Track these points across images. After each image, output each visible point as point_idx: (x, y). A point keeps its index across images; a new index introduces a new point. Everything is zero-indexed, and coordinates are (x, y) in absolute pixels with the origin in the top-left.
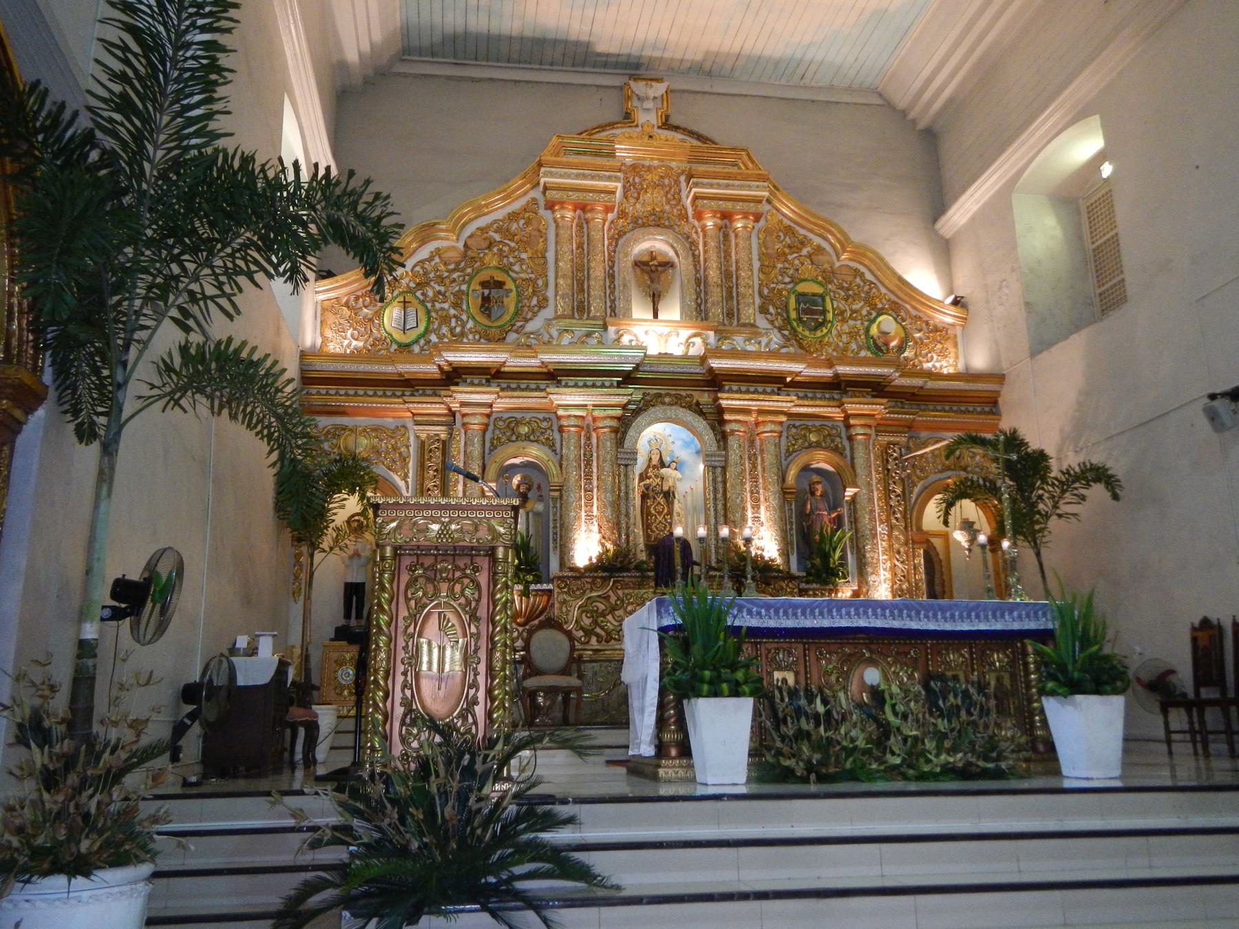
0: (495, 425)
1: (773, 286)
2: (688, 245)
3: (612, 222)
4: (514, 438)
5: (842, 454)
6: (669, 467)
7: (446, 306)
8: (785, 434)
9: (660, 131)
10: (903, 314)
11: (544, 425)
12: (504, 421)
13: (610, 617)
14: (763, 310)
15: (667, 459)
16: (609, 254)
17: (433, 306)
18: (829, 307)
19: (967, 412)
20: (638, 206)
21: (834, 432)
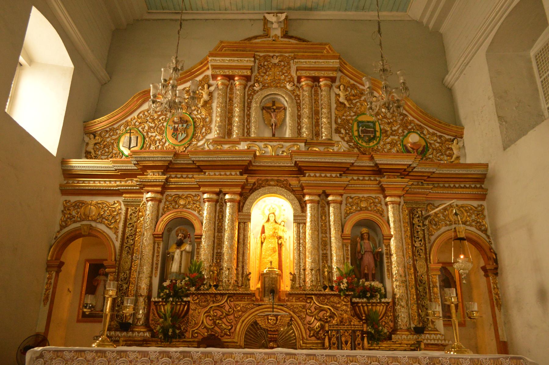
0: (166, 199)
1: (343, 117)
2: (293, 97)
3: (250, 86)
4: (177, 206)
5: (381, 214)
6: (280, 224)
7: (154, 134)
8: (344, 202)
9: (282, 39)
10: (425, 132)
11: (196, 198)
12: (172, 197)
13: (224, 320)
14: (338, 131)
15: (279, 221)
16: (248, 103)
17: (148, 134)
18: (378, 128)
19: (465, 187)
20: (266, 77)
21: (377, 200)
